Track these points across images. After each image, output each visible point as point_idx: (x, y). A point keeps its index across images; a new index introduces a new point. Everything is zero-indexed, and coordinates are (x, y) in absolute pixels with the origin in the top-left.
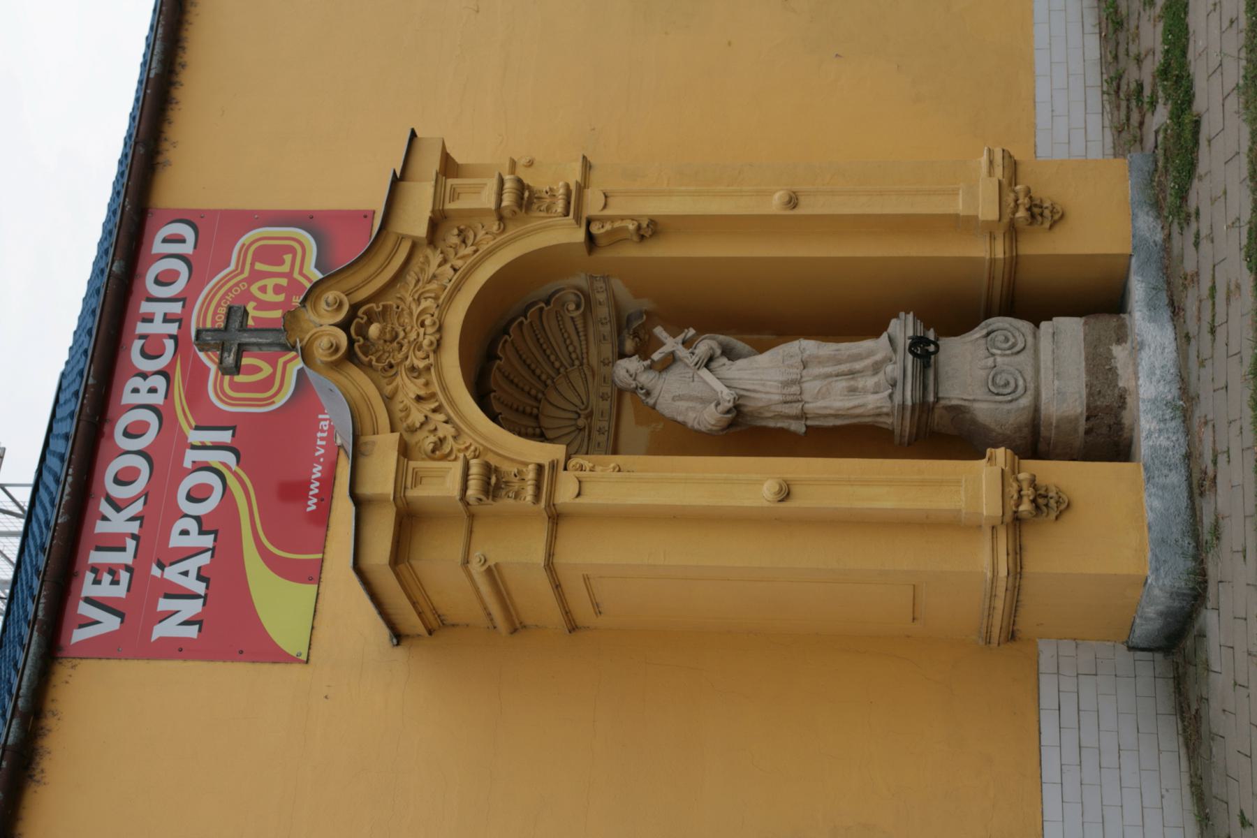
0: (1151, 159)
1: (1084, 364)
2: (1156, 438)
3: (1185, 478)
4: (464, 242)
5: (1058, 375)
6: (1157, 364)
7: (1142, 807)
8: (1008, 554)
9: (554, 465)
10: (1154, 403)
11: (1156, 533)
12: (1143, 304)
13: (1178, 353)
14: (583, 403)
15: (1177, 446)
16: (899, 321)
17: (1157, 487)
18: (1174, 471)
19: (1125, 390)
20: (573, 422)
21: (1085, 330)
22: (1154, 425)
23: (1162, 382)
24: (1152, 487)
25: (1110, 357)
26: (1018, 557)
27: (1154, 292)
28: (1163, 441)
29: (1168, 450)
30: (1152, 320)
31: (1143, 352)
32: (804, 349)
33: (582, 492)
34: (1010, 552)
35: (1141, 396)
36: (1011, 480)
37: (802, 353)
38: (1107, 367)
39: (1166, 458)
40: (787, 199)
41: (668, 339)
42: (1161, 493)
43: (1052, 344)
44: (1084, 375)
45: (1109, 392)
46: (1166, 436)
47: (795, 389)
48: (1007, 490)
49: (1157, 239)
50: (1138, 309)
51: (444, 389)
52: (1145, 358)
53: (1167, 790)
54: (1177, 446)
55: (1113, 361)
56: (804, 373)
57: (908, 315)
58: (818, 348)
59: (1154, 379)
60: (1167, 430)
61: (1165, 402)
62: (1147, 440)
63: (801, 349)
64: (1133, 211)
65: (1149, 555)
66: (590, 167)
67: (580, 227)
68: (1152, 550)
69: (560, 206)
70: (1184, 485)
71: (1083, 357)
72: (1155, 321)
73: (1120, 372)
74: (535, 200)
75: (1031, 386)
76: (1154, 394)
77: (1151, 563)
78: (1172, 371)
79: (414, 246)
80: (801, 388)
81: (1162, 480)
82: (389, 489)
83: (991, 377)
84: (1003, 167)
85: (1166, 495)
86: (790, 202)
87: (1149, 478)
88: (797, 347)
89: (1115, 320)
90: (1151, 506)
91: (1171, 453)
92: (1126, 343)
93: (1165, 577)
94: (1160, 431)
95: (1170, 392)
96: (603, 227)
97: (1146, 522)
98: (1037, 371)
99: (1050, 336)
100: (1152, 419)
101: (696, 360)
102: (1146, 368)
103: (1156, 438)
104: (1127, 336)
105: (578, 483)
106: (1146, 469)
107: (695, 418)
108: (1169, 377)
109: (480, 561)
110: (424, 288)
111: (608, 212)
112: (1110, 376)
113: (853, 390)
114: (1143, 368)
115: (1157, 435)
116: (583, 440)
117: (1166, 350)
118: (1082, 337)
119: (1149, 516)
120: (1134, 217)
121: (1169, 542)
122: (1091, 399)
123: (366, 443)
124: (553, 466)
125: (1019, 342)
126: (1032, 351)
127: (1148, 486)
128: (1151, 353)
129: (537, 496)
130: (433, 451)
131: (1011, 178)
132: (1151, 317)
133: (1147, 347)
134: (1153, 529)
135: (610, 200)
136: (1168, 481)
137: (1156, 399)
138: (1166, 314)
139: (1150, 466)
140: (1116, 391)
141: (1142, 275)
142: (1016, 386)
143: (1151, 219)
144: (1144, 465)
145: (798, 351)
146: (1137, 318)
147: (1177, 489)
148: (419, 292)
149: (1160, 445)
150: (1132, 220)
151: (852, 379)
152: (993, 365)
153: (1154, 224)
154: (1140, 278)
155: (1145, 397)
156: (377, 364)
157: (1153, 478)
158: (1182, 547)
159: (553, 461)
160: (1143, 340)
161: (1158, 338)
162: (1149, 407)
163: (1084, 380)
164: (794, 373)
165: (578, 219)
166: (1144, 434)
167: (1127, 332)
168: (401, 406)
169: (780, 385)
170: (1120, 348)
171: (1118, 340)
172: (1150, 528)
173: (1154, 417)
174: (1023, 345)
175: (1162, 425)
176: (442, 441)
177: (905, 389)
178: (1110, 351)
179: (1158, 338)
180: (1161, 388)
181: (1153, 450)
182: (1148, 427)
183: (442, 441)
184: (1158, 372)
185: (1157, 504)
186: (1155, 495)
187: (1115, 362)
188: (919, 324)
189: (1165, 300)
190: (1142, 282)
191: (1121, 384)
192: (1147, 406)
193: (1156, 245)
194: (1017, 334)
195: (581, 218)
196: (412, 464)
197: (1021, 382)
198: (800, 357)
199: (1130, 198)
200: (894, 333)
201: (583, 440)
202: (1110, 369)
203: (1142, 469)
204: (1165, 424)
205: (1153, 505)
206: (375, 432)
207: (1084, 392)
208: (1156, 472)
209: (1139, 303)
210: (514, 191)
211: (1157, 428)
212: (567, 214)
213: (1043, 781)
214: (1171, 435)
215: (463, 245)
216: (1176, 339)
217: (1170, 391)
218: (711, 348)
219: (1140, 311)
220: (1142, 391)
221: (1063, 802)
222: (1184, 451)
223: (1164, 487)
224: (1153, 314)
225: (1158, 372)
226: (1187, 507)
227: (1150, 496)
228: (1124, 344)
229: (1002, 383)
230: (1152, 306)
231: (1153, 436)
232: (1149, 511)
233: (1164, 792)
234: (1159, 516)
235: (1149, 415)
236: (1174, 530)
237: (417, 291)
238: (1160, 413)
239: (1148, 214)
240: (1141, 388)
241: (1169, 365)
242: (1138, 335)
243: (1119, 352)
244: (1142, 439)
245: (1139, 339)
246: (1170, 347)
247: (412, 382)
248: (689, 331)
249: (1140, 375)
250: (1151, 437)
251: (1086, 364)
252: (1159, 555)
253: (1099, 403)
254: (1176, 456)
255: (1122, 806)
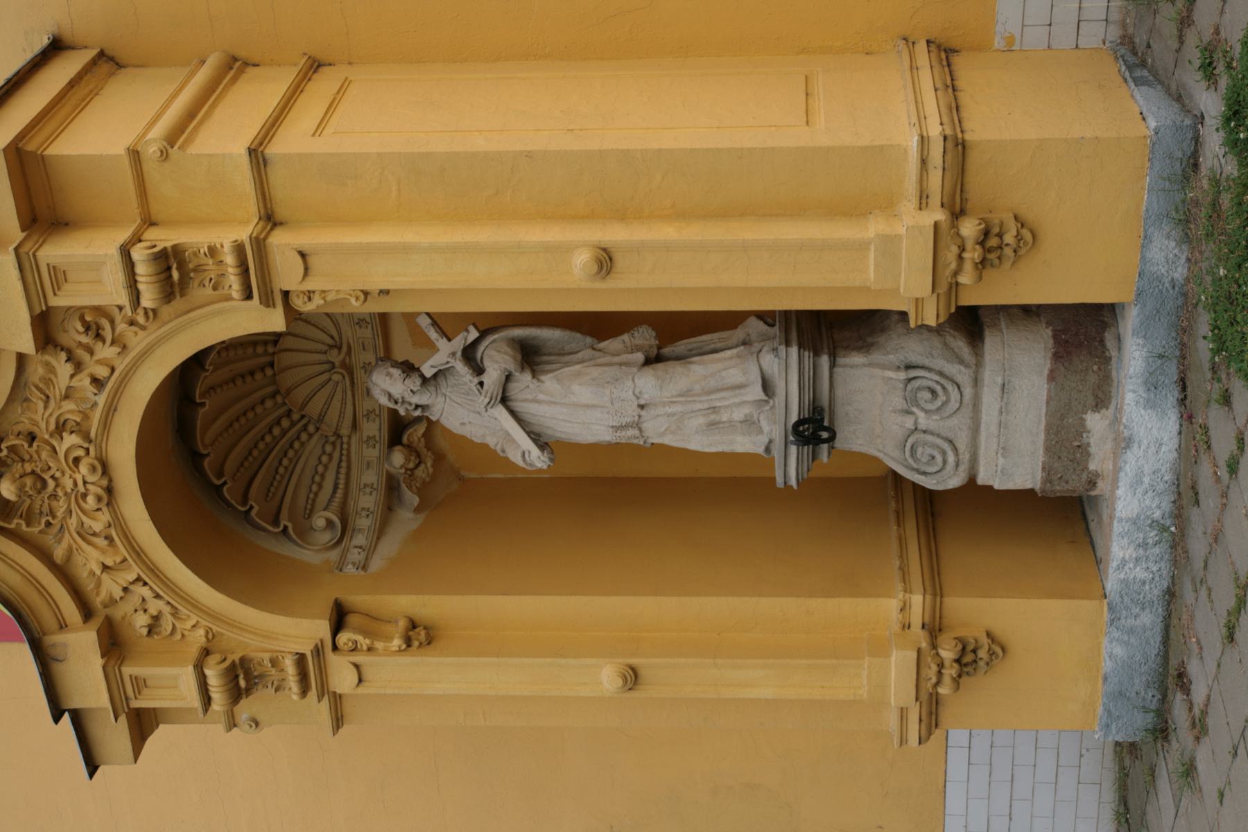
0: (1190, 135)
1: (1042, 436)
2: (1130, 569)
3: (1161, 619)
4: (99, 336)
5: (1005, 450)
6: (1147, 470)
7: (1057, 766)
8: (920, 720)
9: (318, 651)
10: (1135, 523)
11: (1112, 685)
12: (1140, 381)
13: (1179, 454)
14: (332, 337)
15: (1157, 579)
16: (777, 360)
17: (1122, 631)
18: (1148, 610)
19: (1097, 475)
20: (323, 357)
21: (1049, 390)
22: (1130, 552)
23: (1150, 493)
24: (1116, 630)
25: (1081, 429)
26: (934, 717)
27: (1159, 362)
28: (1140, 573)
29: (1144, 583)
30: (1149, 404)
31: (1128, 453)
32: (640, 393)
33: (364, 677)
34: (924, 718)
35: (1118, 514)
36: (929, 659)
37: (638, 398)
38: (1076, 444)
39: (1139, 594)
40: (595, 268)
41: (440, 340)
42: (1126, 638)
43: (999, 400)
44: (1041, 452)
45: (1074, 477)
46: (1144, 566)
47: (631, 432)
48: (923, 673)
49: (1176, 275)
50: (1131, 387)
51: (138, 554)
52: (1132, 461)
53: (1088, 750)
54: (1157, 579)
55: (1084, 435)
56: (643, 413)
57: (789, 349)
58: (661, 388)
59: (1140, 490)
60: (1147, 558)
61: (1150, 521)
62: (1118, 571)
63: (637, 393)
64: (1145, 231)
65: (1100, 710)
66: (265, 160)
67: (274, 306)
68: (1104, 704)
69: (233, 282)
70: (1159, 628)
71: (1042, 427)
72: (1153, 407)
73: (1092, 450)
74: (192, 275)
75: (965, 457)
76: (1136, 511)
77: (1101, 718)
78: (1166, 478)
79: (21, 358)
80: (640, 430)
81: (1131, 622)
82: (104, 701)
83: (909, 445)
84: (944, 169)
85: (1133, 640)
86: (601, 268)
87: (1113, 620)
88: (630, 393)
89: (1095, 368)
90: (1112, 653)
91: (1147, 587)
92: (1107, 409)
93: (1117, 733)
94: (1137, 560)
95: (1159, 507)
96: (310, 299)
97: (1102, 672)
98: (975, 430)
99: (998, 390)
100: (1129, 544)
101: (487, 400)
102: (1130, 474)
103: (1130, 569)
104: (1110, 398)
105: (355, 670)
106: (1111, 608)
107: (496, 445)
108: (1161, 487)
109: (251, 726)
110: (60, 408)
111: (310, 285)
112: (1078, 455)
113: (712, 425)
114: (1126, 474)
115: (1131, 565)
116: (344, 391)
117: (1163, 449)
118: (1045, 398)
119: (1107, 665)
120: (1147, 238)
121: (1128, 694)
122: (1048, 485)
123: (54, 645)
124: (318, 651)
125: (953, 398)
126: (970, 406)
127: (1111, 629)
128: (1141, 454)
129: (304, 692)
130: (149, 632)
131: (957, 182)
132: (1148, 401)
133: (1136, 445)
134: (1109, 680)
135: (312, 261)
136: (1138, 622)
137: (1138, 516)
138: (1173, 395)
139: (1117, 604)
140: (1084, 476)
141: (1144, 337)
142: (945, 462)
143: (1173, 244)
144: (1108, 604)
145: (634, 398)
146: (1127, 401)
147: (1148, 633)
148: (55, 416)
149: (1135, 578)
150: (1143, 246)
151: (714, 412)
152: (913, 428)
153: (1176, 251)
154: (1140, 341)
155: (1124, 515)
156: (29, 530)
157: (1119, 619)
158: (1144, 699)
159: (316, 646)
160: (1131, 435)
161: (1155, 431)
162: (1126, 528)
163: (1041, 459)
164: (631, 413)
165: (267, 301)
166: (1114, 564)
167: (1110, 392)
168: (85, 574)
169: (610, 430)
170: (1097, 416)
171: (1097, 405)
172: (1105, 679)
173: (1132, 542)
174: (957, 405)
175: (1141, 551)
176: (156, 618)
177: (788, 463)
178: (1083, 420)
179: (1155, 431)
180: (1147, 502)
181: (1124, 585)
182: (1121, 555)
183: (156, 618)
184: (1146, 480)
185: (1119, 650)
186: (1117, 640)
187: (1088, 437)
188: (806, 359)
189: (1172, 371)
190: (1143, 346)
191: (1092, 467)
192: (1122, 527)
193: (1174, 287)
194: (950, 387)
195: (272, 292)
196: (128, 670)
197: (951, 458)
198: (636, 404)
199: (1144, 209)
200: (770, 372)
201: (344, 391)
202: (1079, 446)
203: (1106, 609)
204: (1146, 550)
205: (1114, 652)
206: (63, 626)
207: (1039, 475)
208: (1124, 612)
209: (1133, 380)
210: (154, 279)
211: (1134, 556)
212: (248, 296)
213: (949, 745)
214: (1151, 565)
215: (100, 344)
216: (1180, 433)
217: (1159, 507)
218: (505, 369)
219: (1134, 392)
220: (1120, 506)
221: (969, 764)
222: (1165, 586)
223: (1131, 631)
224: (1152, 395)
225: (1146, 480)
226: (1158, 654)
227: (1111, 642)
228: (1103, 411)
229: (924, 460)
230: (1152, 384)
231: (1126, 567)
232: (1108, 659)
233: (1084, 751)
234: (1120, 665)
235: (1126, 540)
236: (1137, 681)
237: (51, 415)
238: (1141, 535)
239: (1168, 237)
240: (1119, 502)
241: (1163, 470)
242: (1125, 427)
243: (1096, 422)
244: (1111, 571)
245: (1126, 433)
246: (1169, 451)
247: (89, 543)
248: (468, 331)
249: (1120, 484)
250: (1123, 568)
251: (1047, 440)
252: (1113, 710)
253: (1058, 488)
254: (1155, 591)
255: (1035, 766)
